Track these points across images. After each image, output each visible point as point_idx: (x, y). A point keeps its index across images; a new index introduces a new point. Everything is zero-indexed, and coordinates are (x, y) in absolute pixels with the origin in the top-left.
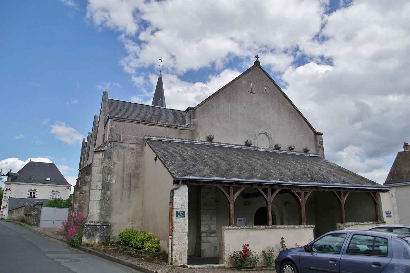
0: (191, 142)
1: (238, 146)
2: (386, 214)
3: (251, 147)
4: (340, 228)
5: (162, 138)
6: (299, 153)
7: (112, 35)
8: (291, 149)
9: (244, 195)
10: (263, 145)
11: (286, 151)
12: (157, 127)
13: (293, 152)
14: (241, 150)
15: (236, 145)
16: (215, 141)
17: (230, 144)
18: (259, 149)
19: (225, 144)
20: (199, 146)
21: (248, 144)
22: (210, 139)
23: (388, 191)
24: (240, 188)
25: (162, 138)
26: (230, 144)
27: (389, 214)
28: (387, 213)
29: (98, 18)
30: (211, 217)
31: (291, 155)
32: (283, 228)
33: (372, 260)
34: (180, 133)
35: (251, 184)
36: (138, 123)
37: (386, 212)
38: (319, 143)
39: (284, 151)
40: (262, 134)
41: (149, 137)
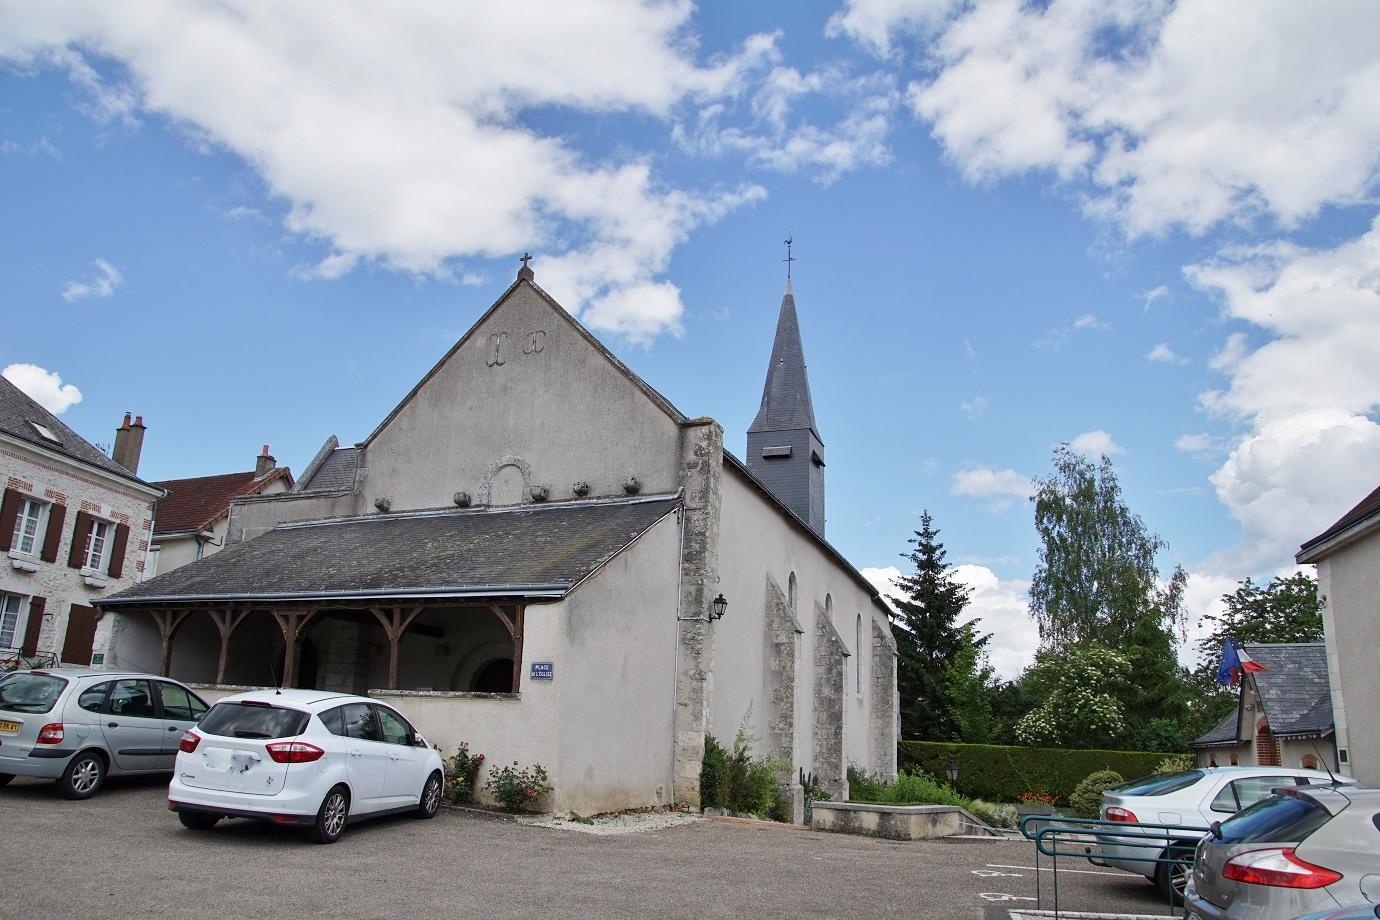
0: (349, 520)
1: (441, 512)
2: (533, 670)
3: (472, 507)
4: (1245, 792)
5: (302, 523)
6: (607, 500)
7: (1032, 187)
8: (582, 493)
9: (414, 628)
10: (507, 496)
11: (566, 500)
12: (299, 502)
13: (590, 498)
14: (443, 520)
15: (438, 509)
16: (395, 510)
17: (423, 510)
18: (492, 511)
19: (415, 511)
20: (364, 525)
21: (463, 503)
22: (382, 508)
23: (561, 599)
24: (181, 611)
25: (302, 523)
26: (423, 510)
27: (542, 671)
28: (537, 667)
29: (974, 169)
30: (344, 681)
31: (582, 510)
32: (229, 690)
33: (380, 804)
34: (333, 505)
35: (256, 603)
36: (270, 501)
37: (534, 666)
38: (696, 453)
39: (560, 501)
40: (507, 469)
41: (284, 525)
